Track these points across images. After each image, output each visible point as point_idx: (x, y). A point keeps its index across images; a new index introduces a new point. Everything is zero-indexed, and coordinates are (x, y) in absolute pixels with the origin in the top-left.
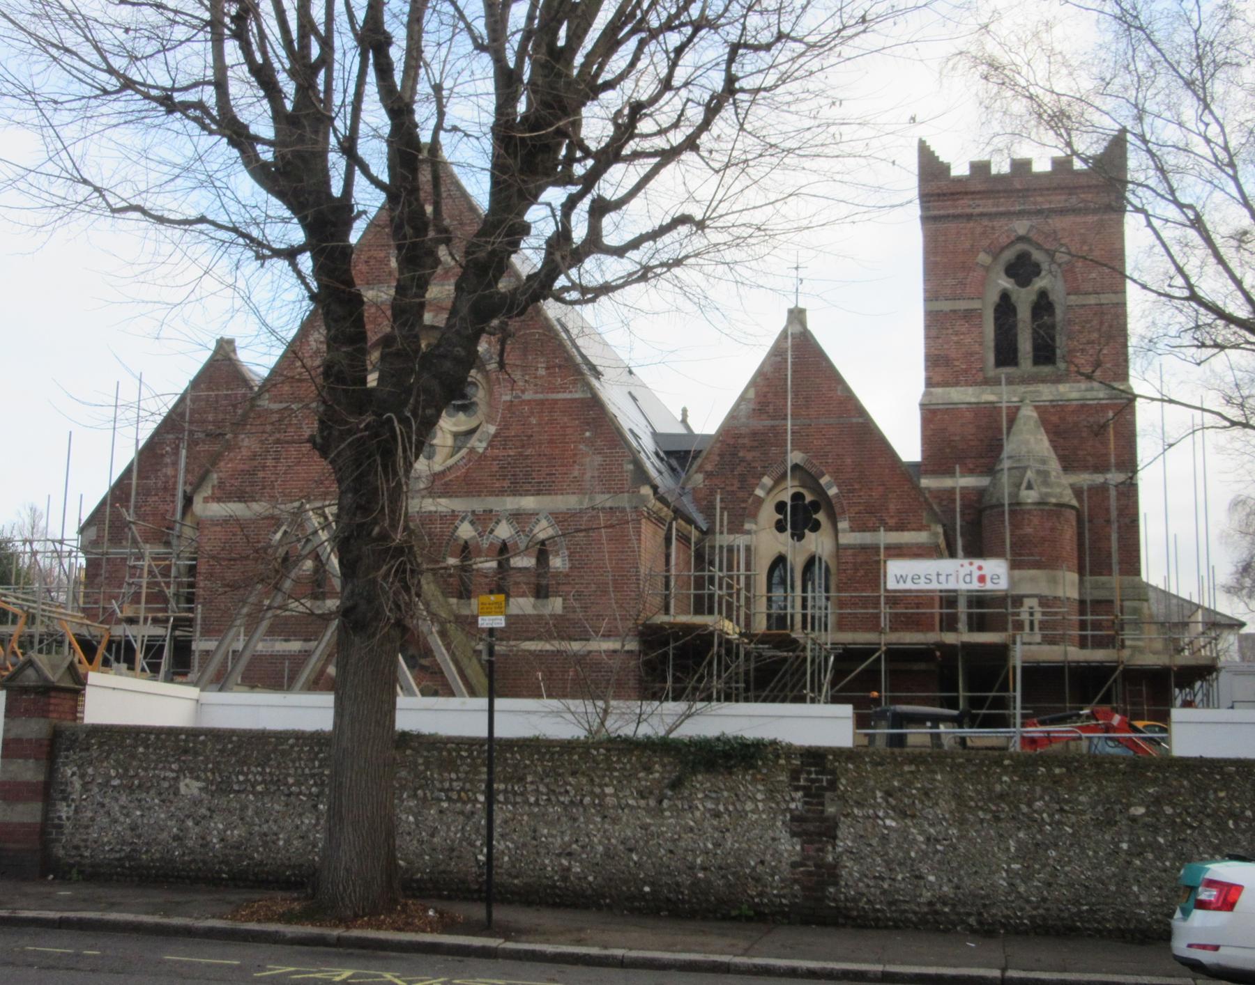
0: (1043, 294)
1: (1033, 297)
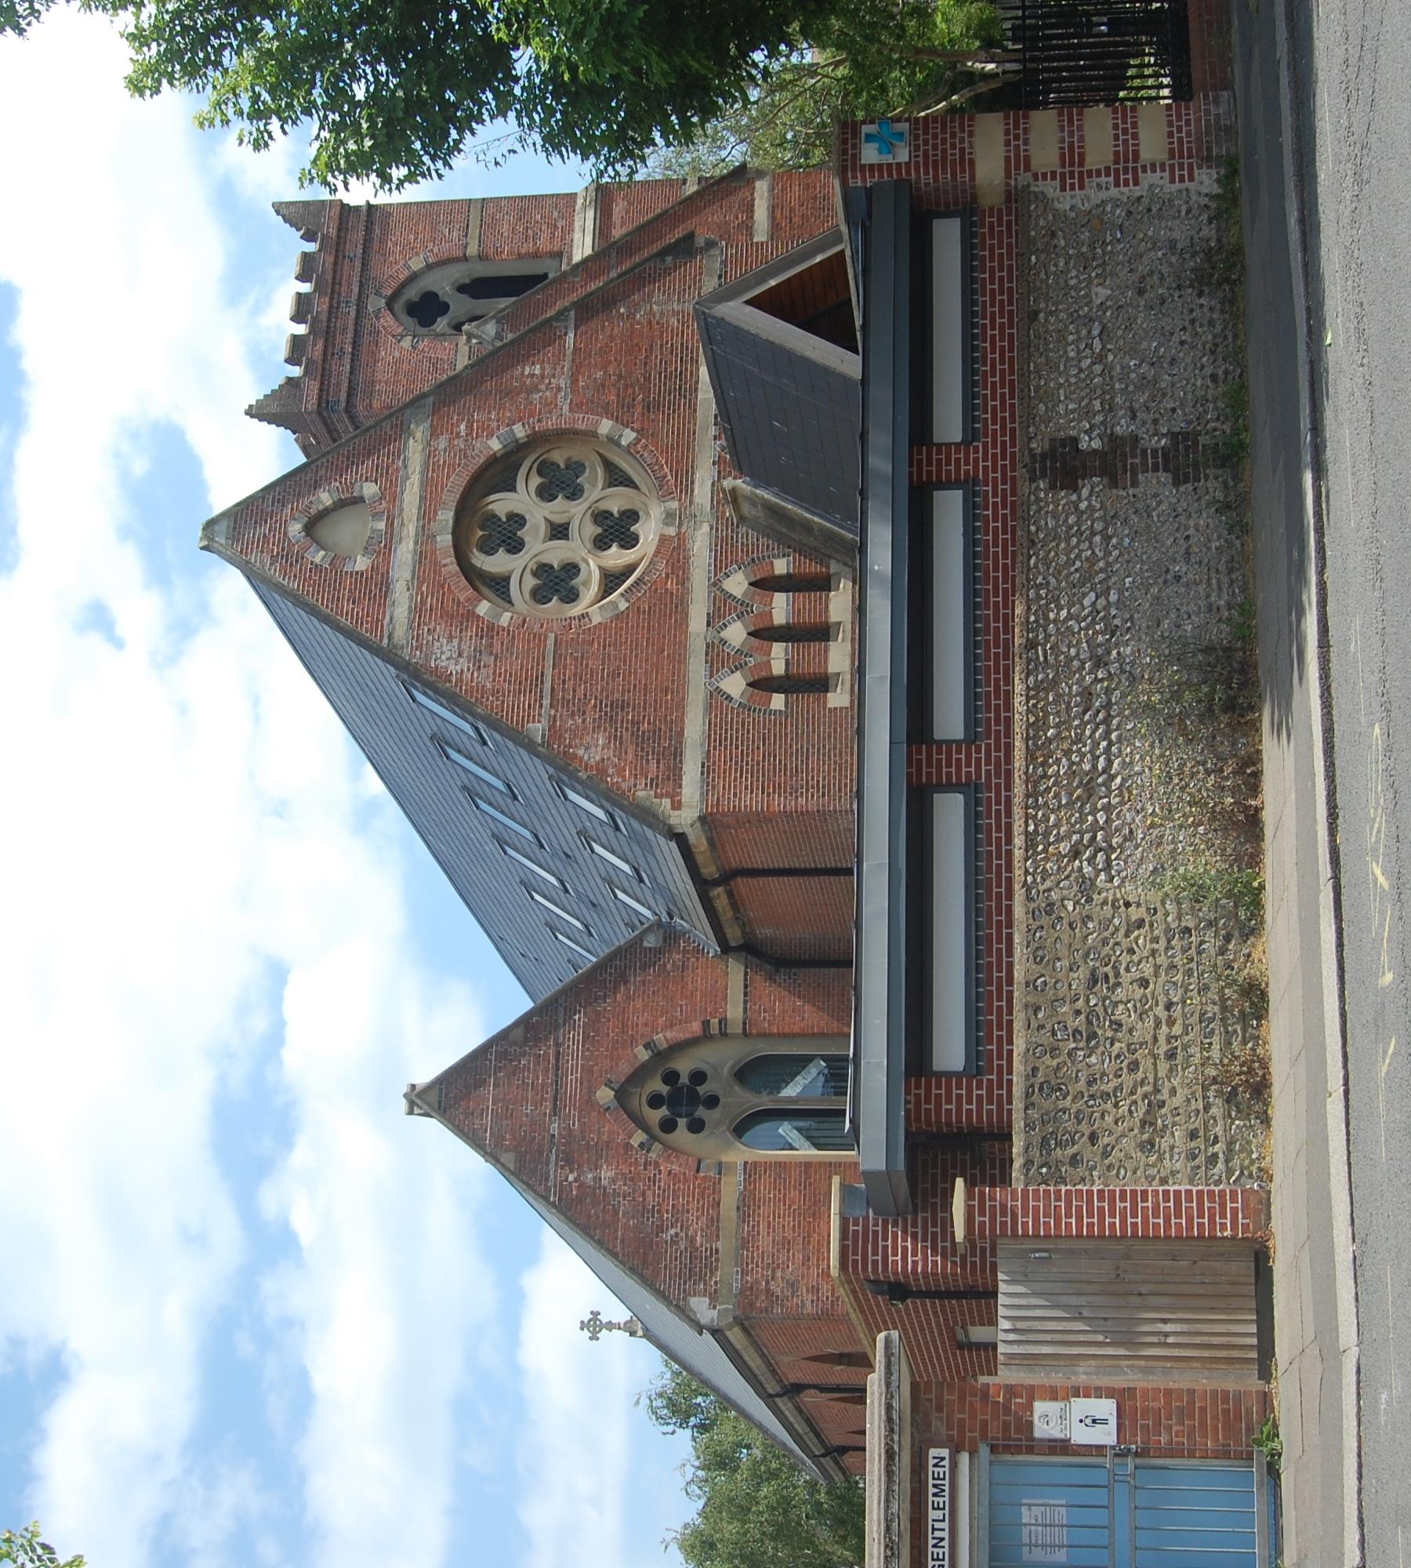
0: (462, 289)
1: (465, 297)
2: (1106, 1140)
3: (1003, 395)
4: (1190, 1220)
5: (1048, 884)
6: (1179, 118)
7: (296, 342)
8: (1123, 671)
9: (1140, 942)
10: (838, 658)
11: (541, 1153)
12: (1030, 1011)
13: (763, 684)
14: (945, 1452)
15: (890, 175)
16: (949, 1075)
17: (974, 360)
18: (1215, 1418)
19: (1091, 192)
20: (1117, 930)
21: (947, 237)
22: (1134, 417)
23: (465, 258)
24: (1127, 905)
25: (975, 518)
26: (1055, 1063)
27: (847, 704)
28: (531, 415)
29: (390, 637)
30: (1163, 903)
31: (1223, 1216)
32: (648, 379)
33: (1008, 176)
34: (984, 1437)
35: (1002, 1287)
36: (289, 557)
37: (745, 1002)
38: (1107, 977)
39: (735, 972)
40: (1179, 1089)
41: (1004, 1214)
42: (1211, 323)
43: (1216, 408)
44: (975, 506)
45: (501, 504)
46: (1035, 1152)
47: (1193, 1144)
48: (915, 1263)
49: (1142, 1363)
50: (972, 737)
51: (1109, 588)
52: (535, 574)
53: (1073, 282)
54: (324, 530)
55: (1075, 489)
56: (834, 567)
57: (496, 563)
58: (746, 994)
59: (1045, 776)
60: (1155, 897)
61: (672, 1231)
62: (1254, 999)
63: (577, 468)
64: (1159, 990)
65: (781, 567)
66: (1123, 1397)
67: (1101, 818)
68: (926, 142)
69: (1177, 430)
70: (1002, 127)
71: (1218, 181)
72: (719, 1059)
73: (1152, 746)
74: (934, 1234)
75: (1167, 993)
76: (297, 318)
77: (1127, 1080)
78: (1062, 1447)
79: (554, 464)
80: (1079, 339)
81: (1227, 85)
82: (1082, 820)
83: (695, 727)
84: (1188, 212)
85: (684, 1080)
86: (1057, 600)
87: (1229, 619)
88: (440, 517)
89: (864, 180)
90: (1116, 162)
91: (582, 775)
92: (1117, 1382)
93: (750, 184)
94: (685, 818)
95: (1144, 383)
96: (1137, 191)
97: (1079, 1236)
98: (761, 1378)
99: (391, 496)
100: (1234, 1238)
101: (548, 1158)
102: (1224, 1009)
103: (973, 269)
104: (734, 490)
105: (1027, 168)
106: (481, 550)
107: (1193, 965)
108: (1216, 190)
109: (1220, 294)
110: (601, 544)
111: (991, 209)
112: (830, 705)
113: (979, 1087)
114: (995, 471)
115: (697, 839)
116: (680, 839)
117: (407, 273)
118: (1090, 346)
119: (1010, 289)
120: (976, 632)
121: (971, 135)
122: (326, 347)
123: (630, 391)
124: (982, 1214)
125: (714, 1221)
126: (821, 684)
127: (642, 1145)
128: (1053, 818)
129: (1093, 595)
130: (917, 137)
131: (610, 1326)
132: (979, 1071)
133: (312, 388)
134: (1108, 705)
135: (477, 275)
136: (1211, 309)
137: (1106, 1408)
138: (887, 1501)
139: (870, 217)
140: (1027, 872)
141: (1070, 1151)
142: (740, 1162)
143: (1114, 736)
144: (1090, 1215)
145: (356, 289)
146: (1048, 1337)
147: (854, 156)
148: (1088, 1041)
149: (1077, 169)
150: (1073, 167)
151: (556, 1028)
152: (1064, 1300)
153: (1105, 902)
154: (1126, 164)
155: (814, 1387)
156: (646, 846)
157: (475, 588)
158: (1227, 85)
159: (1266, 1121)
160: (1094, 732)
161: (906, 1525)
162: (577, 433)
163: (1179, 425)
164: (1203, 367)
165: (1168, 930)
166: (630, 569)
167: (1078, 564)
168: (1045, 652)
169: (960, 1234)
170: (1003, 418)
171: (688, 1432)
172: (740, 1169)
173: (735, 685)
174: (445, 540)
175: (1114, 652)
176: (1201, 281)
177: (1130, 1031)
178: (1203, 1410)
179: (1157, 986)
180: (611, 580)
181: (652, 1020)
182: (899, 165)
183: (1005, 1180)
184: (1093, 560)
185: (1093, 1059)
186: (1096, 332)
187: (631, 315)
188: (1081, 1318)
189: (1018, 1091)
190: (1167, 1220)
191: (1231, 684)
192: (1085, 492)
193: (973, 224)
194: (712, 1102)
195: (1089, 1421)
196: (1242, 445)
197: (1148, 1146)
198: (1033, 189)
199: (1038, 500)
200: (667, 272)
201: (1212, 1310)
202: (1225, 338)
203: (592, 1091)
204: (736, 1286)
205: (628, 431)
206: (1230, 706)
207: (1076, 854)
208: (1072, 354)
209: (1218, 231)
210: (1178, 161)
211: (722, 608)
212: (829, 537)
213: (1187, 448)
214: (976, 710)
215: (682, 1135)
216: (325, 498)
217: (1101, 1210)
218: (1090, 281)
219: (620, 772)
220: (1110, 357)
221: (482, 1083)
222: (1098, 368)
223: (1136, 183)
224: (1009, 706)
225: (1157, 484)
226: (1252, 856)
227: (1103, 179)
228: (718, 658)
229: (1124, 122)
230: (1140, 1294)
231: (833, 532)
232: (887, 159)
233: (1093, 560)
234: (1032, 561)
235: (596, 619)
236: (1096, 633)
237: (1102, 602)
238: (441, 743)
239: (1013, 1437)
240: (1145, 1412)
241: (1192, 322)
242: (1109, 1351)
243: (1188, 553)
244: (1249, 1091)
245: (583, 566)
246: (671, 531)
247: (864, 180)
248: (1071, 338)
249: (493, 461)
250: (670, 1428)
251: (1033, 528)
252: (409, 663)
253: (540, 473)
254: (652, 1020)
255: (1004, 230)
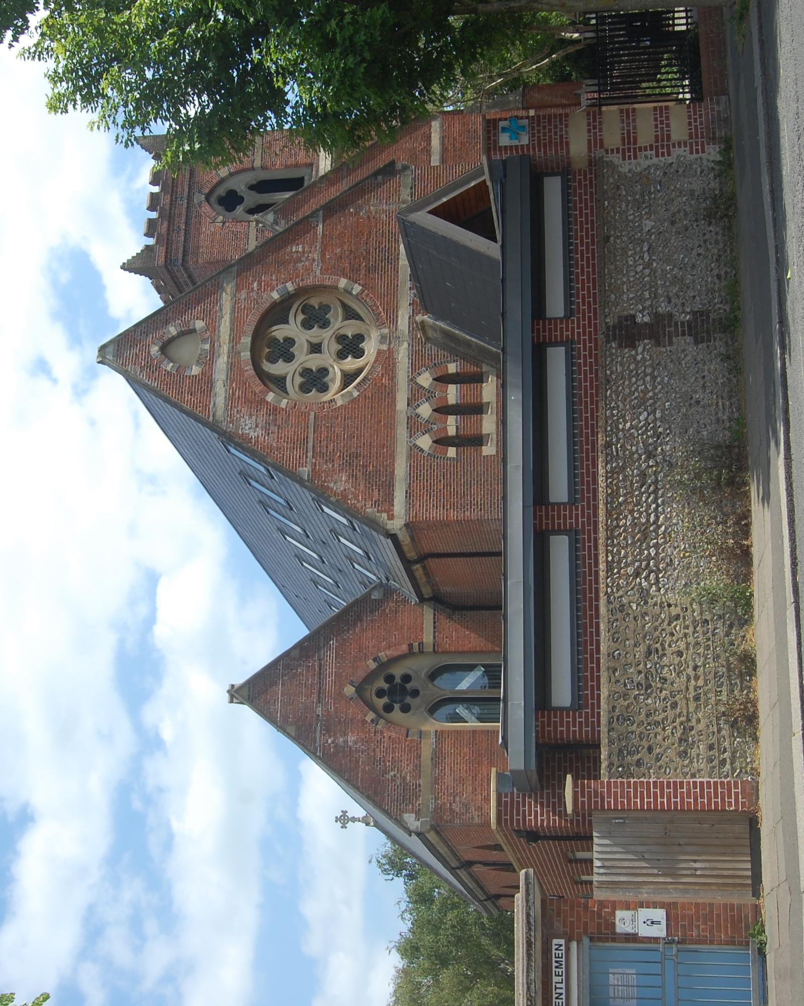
0: (252, 188)
1: (253, 193)
2: (658, 751)
3: (589, 287)
4: (709, 800)
5: (621, 593)
6: (695, 114)
7: (151, 223)
8: (665, 461)
9: (678, 628)
10: (488, 424)
11: (311, 726)
12: (611, 672)
13: (443, 441)
14: (562, 942)
15: (517, 152)
16: (562, 709)
17: (571, 266)
18: (726, 920)
19: (641, 161)
20: (663, 621)
21: (553, 188)
22: (670, 302)
23: (253, 169)
24: (669, 605)
25: (573, 364)
26: (626, 703)
27: (494, 452)
28: (297, 277)
29: (214, 416)
30: (691, 604)
31: (730, 797)
32: (368, 253)
33: (590, 151)
34: (586, 933)
35: (596, 840)
36: (151, 367)
37: (434, 632)
38: (657, 650)
39: (428, 614)
40: (702, 720)
41: (596, 796)
42: (717, 242)
43: (720, 296)
44: (572, 357)
45: (280, 332)
46: (615, 759)
47: (711, 753)
48: (542, 821)
49: (681, 887)
50: (573, 501)
51: (656, 409)
52: (301, 375)
53: (631, 217)
54: (173, 350)
55: (634, 347)
56: (485, 368)
57: (278, 368)
58: (435, 628)
59: (618, 526)
60: (686, 601)
61: (392, 773)
62: (747, 664)
63: (326, 308)
64: (689, 658)
65: (452, 368)
66: (670, 908)
67: (653, 552)
68: (539, 131)
69: (696, 309)
70: (585, 122)
71: (720, 152)
72: (419, 666)
73: (683, 507)
74: (554, 803)
75: (694, 660)
76: (151, 208)
77: (670, 714)
78: (633, 938)
79: (311, 306)
80: (635, 253)
81: (724, 92)
82: (641, 553)
83: (401, 468)
84: (702, 172)
85: (398, 680)
86: (624, 417)
87: (730, 427)
88: (243, 340)
89: (501, 155)
90: (657, 141)
91: (333, 499)
92: (666, 898)
93: (428, 123)
94: (396, 525)
95: (676, 280)
96: (670, 160)
97: (642, 809)
98: (448, 859)
99: (212, 327)
100: (736, 810)
101: (315, 729)
102: (729, 670)
103: (569, 208)
104: (422, 322)
105: (602, 146)
106: (269, 360)
107: (710, 643)
108: (718, 158)
109: (722, 224)
110: (341, 355)
111: (580, 170)
112: (484, 454)
113: (580, 717)
114: (584, 335)
115: (404, 538)
116: (393, 537)
117: (218, 179)
118: (642, 258)
119: (592, 221)
120: (574, 435)
121: (566, 126)
122: (169, 226)
123: (357, 260)
124: (583, 796)
125: (417, 768)
126: (478, 441)
127: (372, 721)
128: (623, 552)
129: (646, 413)
130: (533, 128)
131: (354, 820)
132: (580, 707)
133: (161, 252)
134: (656, 482)
135: (260, 179)
136: (716, 234)
137: (660, 914)
138: (528, 972)
139: (505, 176)
140: (607, 586)
141: (636, 757)
142: (433, 730)
143: (660, 501)
144: (649, 797)
145: (187, 190)
146: (624, 871)
147: (495, 141)
148: (646, 690)
149: (632, 146)
150: (630, 145)
151: (319, 649)
152: (633, 848)
153: (655, 604)
154: (662, 142)
155: (480, 863)
156: (373, 541)
157: (265, 385)
158: (724, 92)
159: (756, 739)
160: (647, 498)
161: (539, 985)
162: (325, 287)
163: (698, 307)
164: (712, 270)
165: (694, 621)
166: (359, 371)
167: (636, 394)
168: (617, 449)
169: (569, 809)
170: (589, 302)
171: (402, 879)
172: (433, 734)
173: (425, 442)
174: (246, 355)
175: (659, 449)
176: (710, 216)
177: (672, 684)
178: (718, 916)
179: (688, 656)
180: (348, 378)
181: (376, 644)
182: (522, 146)
183: (597, 777)
184: (645, 392)
185: (650, 701)
186: (645, 249)
187: (357, 213)
188: (643, 859)
189: (604, 720)
190: (696, 800)
191: (729, 469)
192: (640, 349)
193: (569, 180)
194: (415, 693)
195: (649, 922)
196: (736, 319)
197: (683, 754)
198: (605, 159)
199: (611, 354)
200: (379, 186)
201: (724, 854)
202: (726, 251)
203: (341, 687)
204: (431, 807)
205: (356, 285)
206: (731, 482)
207: (637, 574)
208: (631, 263)
209: (720, 183)
210: (695, 140)
211: (416, 395)
212: (482, 350)
213: (703, 321)
214: (575, 484)
215: (397, 714)
216: (173, 330)
217: (655, 794)
218: (641, 217)
219: (356, 497)
220: (655, 265)
221: (275, 683)
222: (647, 271)
223: (669, 155)
224: (595, 481)
225: (684, 343)
226: (745, 575)
227: (649, 152)
228: (415, 426)
229: (661, 116)
230: (679, 845)
231: (484, 347)
232: (515, 143)
233: (645, 392)
234: (608, 393)
235: (340, 403)
236: (648, 437)
237: (651, 417)
238: (246, 476)
239: (603, 932)
240: (683, 917)
241: (705, 241)
242: (661, 879)
243: (704, 387)
244: (746, 720)
245: (331, 370)
246: (384, 347)
247: (501, 155)
248: (630, 253)
249: (275, 305)
250: (391, 877)
251: (608, 372)
252: (225, 432)
253: (303, 312)
254: (376, 644)
255: (588, 184)
